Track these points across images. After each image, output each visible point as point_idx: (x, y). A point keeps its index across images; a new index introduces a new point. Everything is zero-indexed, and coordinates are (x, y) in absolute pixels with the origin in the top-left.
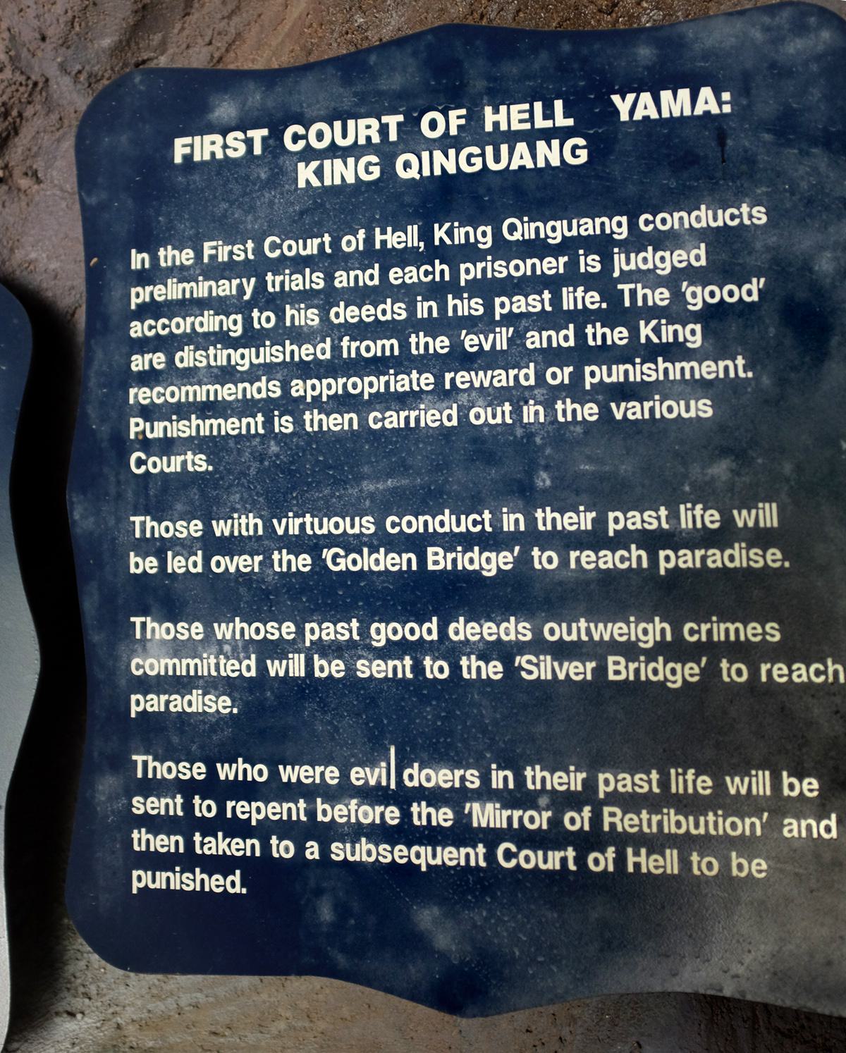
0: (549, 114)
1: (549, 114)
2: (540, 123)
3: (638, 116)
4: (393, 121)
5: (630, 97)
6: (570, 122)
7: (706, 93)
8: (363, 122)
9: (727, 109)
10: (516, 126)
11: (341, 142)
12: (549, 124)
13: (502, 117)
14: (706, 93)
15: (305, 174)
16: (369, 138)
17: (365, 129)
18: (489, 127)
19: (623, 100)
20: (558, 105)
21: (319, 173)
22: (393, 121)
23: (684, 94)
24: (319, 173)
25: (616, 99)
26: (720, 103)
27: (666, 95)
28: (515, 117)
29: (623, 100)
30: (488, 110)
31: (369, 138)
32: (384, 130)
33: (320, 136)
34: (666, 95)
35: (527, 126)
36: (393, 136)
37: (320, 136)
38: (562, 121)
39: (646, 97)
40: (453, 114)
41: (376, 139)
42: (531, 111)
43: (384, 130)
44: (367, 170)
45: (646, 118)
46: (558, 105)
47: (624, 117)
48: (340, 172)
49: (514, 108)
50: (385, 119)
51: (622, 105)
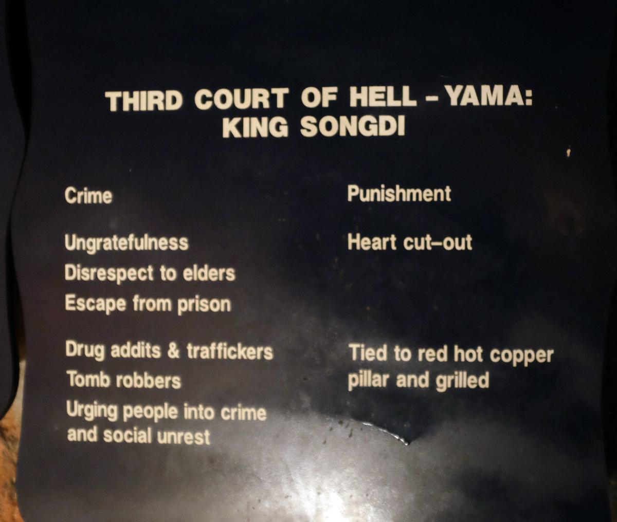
0: (398, 96)
1: (398, 96)
2: (392, 103)
3: (464, 103)
4: (281, 93)
5: (459, 88)
7: (515, 89)
8: (257, 91)
9: (529, 102)
10: (373, 104)
11: (239, 106)
12: (397, 104)
13: (363, 96)
14: (515, 89)
16: (261, 104)
18: (353, 104)
19: (454, 88)
20: (406, 90)
22: (281, 93)
23: (499, 89)
25: (448, 88)
26: (524, 98)
27: (485, 89)
28: (373, 96)
29: (454, 88)
30: (353, 90)
31: (261, 104)
32: (273, 99)
34: (485, 89)
35: (382, 104)
36: (280, 104)
37: (223, 99)
38: (408, 102)
39: (470, 89)
40: (326, 90)
41: (266, 105)
42: (386, 93)
43: (273, 99)
45: (470, 105)
46: (406, 90)
47: (454, 103)
49: (373, 89)
50: (274, 91)
51: (453, 93)
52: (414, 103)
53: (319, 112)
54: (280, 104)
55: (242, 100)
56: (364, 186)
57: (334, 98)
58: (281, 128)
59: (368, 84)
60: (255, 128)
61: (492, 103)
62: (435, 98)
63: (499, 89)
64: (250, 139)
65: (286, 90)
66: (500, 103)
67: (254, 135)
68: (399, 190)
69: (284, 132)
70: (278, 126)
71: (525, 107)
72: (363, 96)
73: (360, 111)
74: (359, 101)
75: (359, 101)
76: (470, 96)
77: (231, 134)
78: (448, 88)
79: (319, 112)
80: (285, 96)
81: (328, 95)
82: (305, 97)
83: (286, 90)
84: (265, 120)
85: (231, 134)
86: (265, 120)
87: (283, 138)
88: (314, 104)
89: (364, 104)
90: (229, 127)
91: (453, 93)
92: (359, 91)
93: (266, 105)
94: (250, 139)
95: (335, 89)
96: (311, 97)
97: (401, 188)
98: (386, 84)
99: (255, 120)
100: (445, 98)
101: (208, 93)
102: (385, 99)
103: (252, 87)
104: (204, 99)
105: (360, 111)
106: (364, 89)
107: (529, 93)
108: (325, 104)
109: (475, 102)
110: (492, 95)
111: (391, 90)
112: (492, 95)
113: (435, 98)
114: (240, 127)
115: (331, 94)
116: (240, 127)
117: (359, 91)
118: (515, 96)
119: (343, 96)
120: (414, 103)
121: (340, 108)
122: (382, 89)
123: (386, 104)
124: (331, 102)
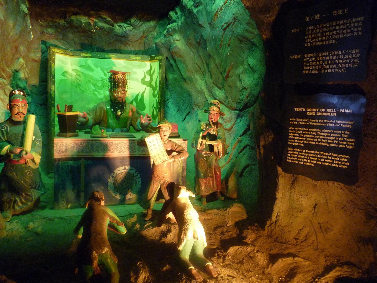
0: (333, 110)
1: (333, 110)
2: (332, 111)
3: (342, 112)
4: (318, 109)
6: (335, 111)
10: (330, 111)
11: (312, 111)
12: (333, 111)
13: (328, 110)
15: (308, 113)
17: (315, 110)
18: (327, 111)
20: (334, 110)
21: (309, 113)
22: (318, 109)
23: (347, 110)
24: (309, 113)
25: (340, 110)
30: (327, 109)
32: (317, 110)
33: (310, 110)
34: (345, 110)
36: (317, 111)
37: (310, 110)
38: (334, 111)
39: (343, 110)
40: (324, 109)
41: (316, 111)
43: (317, 110)
44: (314, 114)
45: (343, 112)
46: (334, 110)
47: (341, 112)
48: (311, 114)
49: (330, 109)
51: (341, 110)
52: (335, 111)
53: (323, 112)
54: (317, 111)
62: (338, 111)
63: (347, 110)
65: (318, 109)
72: (328, 110)
73: (328, 112)
78: (340, 110)
79: (323, 112)
81: (324, 110)
82: (321, 110)
83: (318, 109)
93: (316, 111)
96: (322, 110)
101: (308, 109)
104: (308, 110)
105: (328, 112)
109: (344, 111)
111: (332, 109)
113: (338, 111)
119: (326, 110)
121: (325, 112)
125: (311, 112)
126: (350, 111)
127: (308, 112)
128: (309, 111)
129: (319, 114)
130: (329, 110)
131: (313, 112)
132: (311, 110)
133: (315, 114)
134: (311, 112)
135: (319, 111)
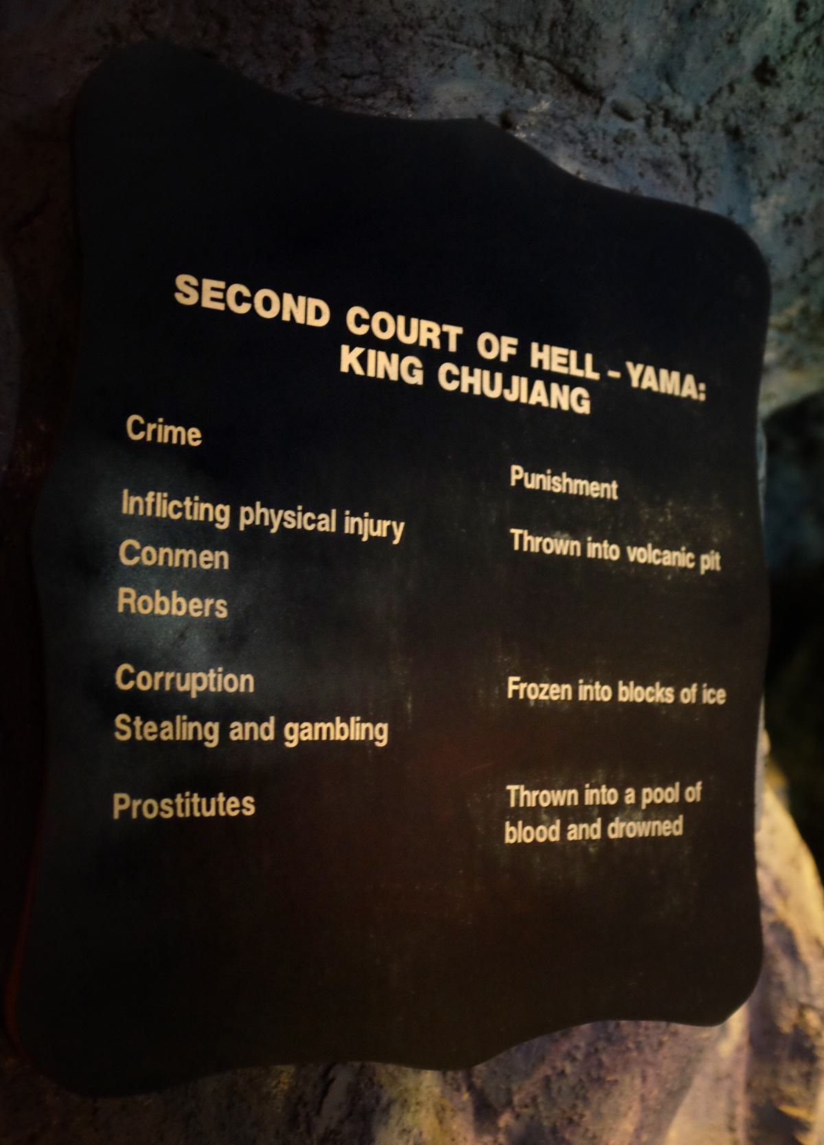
0: (581, 365)
1: (581, 365)
2: (575, 372)
3: (645, 386)
4: (454, 331)
8: (425, 324)
10: (556, 369)
11: (403, 338)
12: (579, 373)
13: (544, 356)
14: (690, 379)
16: (429, 342)
17: (425, 332)
18: (534, 364)
20: (589, 358)
22: (454, 331)
23: (676, 375)
25: (630, 365)
27: (664, 373)
28: (556, 360)
29: (635, 365)
30: (535, 346)
31: (429, 342)
32: (444, 337)
35: (564, 370)
36: (453, 347)
37: (383, 325)
40: (506, 340)
41: (436, 345)
42: (568, 357)
43: (444, 337)
45: (649, 389)
46: (589, 358)
47: (635, 384)
49: (557, 350)
50: (446, 328)
51: (635, 371)
52: (596, 376)
53: (493, 366)
54: (453, 347)
55: (408, 332)
56: (530, 469)
57: (513, 351)
58: (415, 372)
59: (552, 344)
60: (382, 365)
61: (670, 392)
64: (375, 379)
65: (460, 330)
66: (677, 393)
67: (381, 375)
68: (566, 480)
69: (418, 379)
70: (411, 368)
71: (697, 401)
74: (540, 362)
75: (540, 362)
76: (649, 382)
77: (350, 367)
78: (630, 365)
79: (493, 366)
80: (458, 336)
81: (505, 347)
83: (460, 330)
84: (395, 357)
85: (350, 367)
86: (395, 357)
87: (416, 385)
88: (491, 356)
89: (546, 367)
90: (349, 358)
91: (635, 371)
92: (541, 350)
93: (436, 345)
94: (375, 379)
95: (514, 341)
96: (488, 346)
97: (568, 476)
98: (570, 348)
99: (382, 355)
100: (626, 377)
102: (567, 365)
103: (421, 317)
106: (546, 348)
107: (702, 387)
108: (504, 359)
110: (669, 383)
111: (573, 354)
112: (669, 383)
114: (363, 360)
115: (510, 346)
116: (363, 360)
117: (541, 350)
118: (690, 389)
120: (596, 376)
121: (518, 365)
122: (564, 351)
123: (569, 371)
124: (510, 356)
125: (393, 347)
126: (690, 389)
127: (354, 341)
128: (369, 341)
129: (466, 380)
130: (549, 357)
131: (414, 350)
132: (393, 326)
133: (418, 379)
134: (393, 347)
135: (468, 356)
